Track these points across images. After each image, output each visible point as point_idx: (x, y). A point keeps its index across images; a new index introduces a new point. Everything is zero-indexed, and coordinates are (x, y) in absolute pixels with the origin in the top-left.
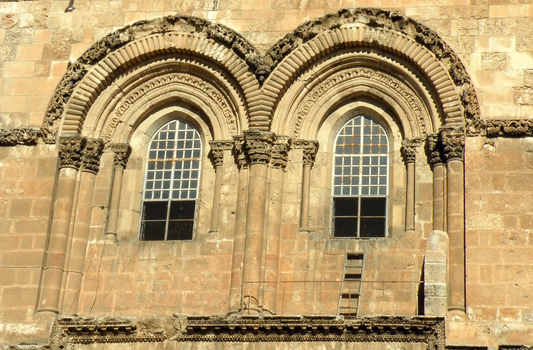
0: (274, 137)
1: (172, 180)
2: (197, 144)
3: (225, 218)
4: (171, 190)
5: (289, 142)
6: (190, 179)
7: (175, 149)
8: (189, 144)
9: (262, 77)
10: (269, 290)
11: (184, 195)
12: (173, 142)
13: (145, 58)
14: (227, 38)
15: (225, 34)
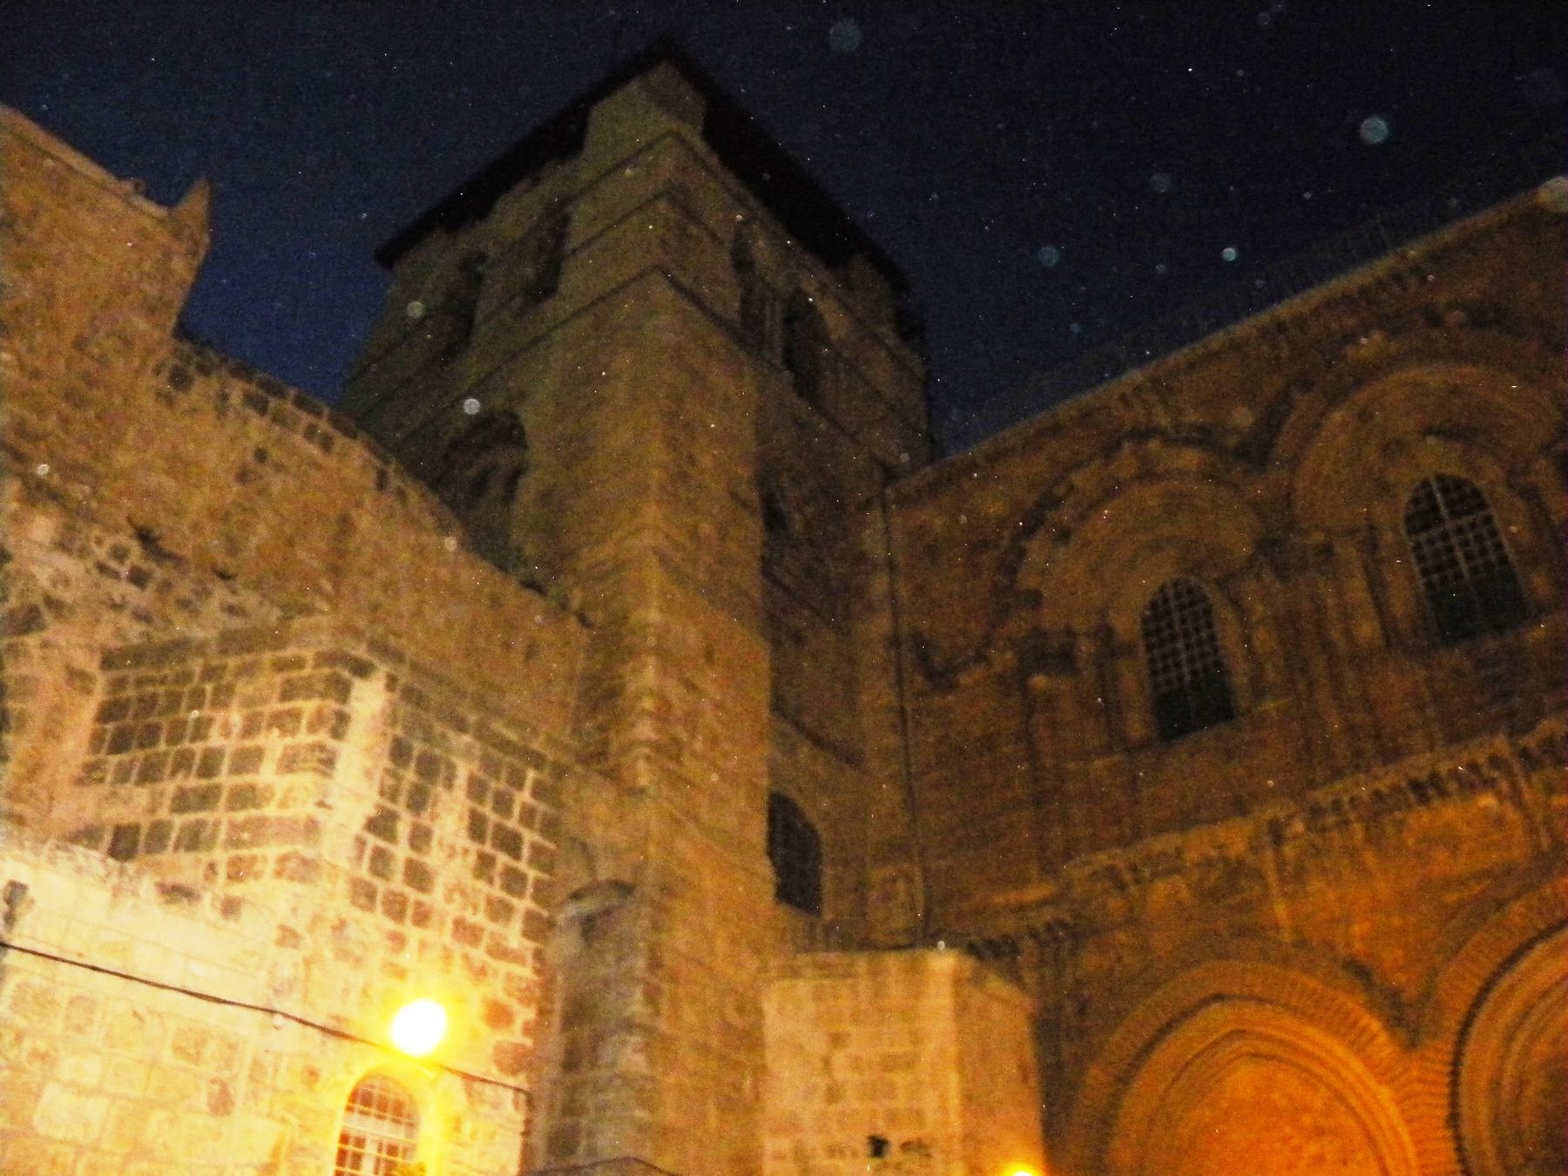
4: (1185, 670)
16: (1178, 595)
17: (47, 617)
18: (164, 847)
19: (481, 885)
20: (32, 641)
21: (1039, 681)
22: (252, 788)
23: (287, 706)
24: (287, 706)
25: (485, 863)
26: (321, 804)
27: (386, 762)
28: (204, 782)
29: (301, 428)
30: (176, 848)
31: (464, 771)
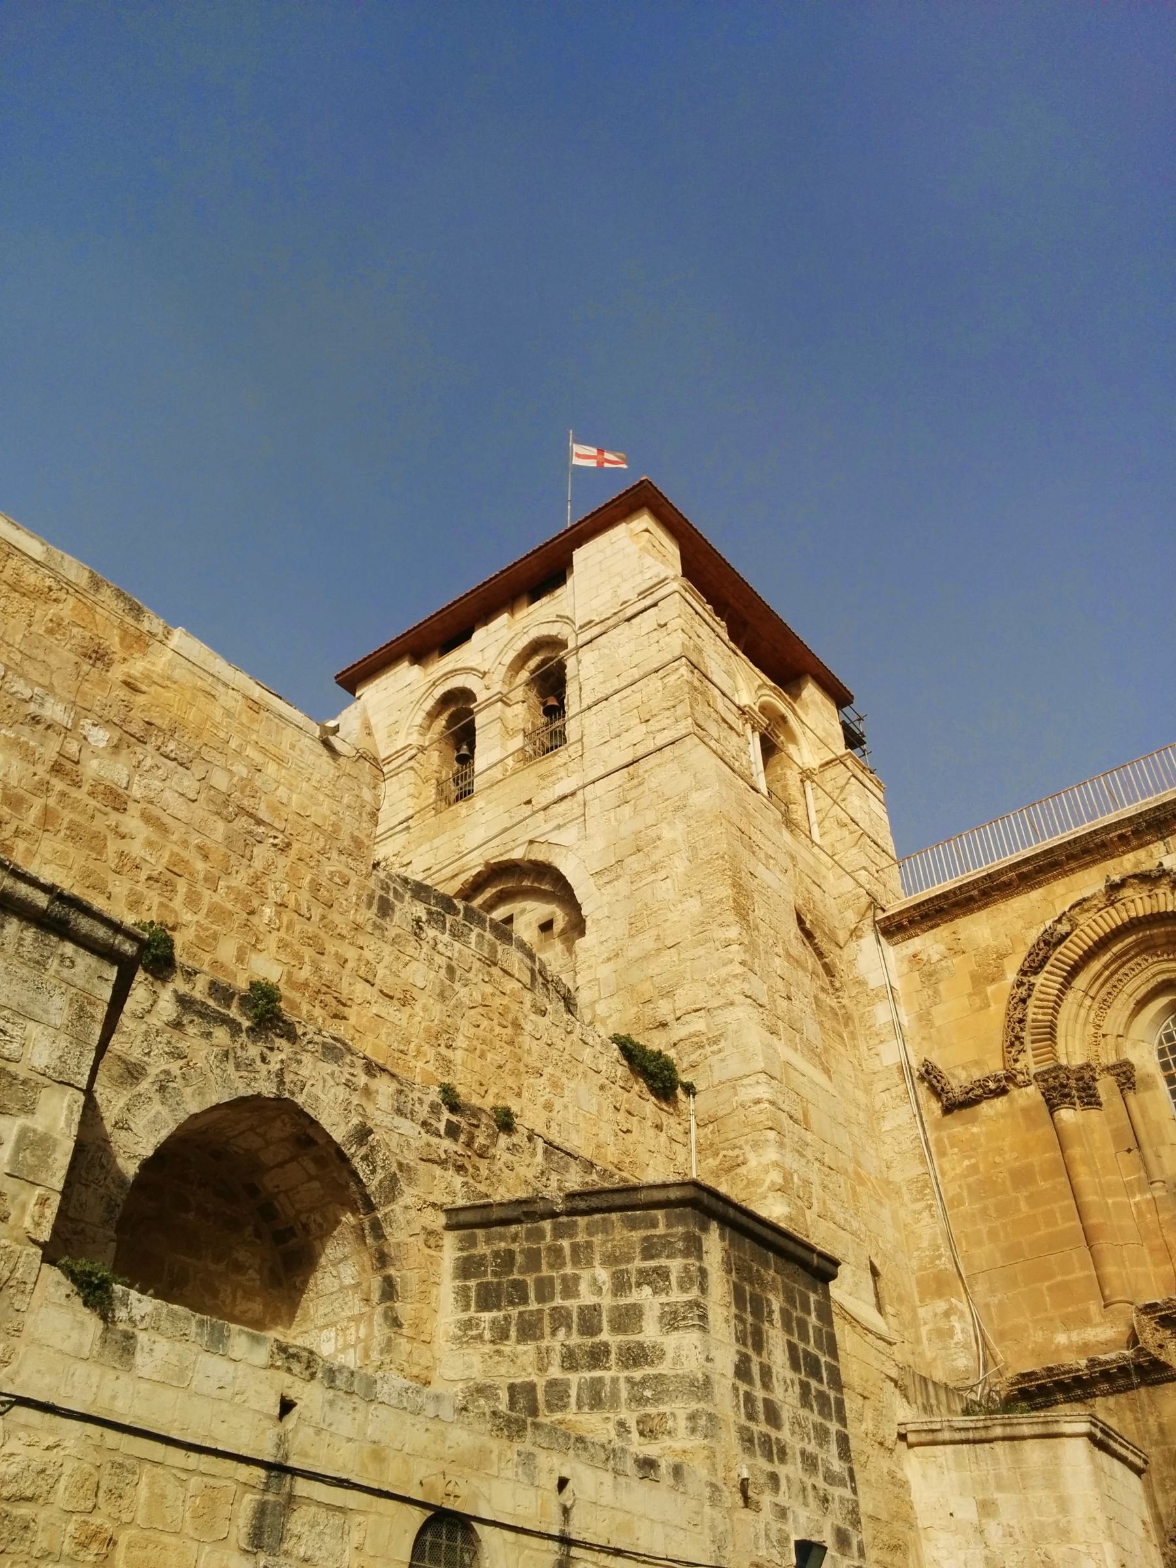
13: (1102, 944)
17: (402, 1183)
18: (565, 1406)
20: (397, 1207)
21: (1066, 1115)
22: (640, 1345)
23: (652, 1263)
24: (652, 1263)
25: (805, 1387)
26: (708, 1359)
27: (733, 1310)
28: (589, 1341)
29: (473, 937)
30: (579, 1408)
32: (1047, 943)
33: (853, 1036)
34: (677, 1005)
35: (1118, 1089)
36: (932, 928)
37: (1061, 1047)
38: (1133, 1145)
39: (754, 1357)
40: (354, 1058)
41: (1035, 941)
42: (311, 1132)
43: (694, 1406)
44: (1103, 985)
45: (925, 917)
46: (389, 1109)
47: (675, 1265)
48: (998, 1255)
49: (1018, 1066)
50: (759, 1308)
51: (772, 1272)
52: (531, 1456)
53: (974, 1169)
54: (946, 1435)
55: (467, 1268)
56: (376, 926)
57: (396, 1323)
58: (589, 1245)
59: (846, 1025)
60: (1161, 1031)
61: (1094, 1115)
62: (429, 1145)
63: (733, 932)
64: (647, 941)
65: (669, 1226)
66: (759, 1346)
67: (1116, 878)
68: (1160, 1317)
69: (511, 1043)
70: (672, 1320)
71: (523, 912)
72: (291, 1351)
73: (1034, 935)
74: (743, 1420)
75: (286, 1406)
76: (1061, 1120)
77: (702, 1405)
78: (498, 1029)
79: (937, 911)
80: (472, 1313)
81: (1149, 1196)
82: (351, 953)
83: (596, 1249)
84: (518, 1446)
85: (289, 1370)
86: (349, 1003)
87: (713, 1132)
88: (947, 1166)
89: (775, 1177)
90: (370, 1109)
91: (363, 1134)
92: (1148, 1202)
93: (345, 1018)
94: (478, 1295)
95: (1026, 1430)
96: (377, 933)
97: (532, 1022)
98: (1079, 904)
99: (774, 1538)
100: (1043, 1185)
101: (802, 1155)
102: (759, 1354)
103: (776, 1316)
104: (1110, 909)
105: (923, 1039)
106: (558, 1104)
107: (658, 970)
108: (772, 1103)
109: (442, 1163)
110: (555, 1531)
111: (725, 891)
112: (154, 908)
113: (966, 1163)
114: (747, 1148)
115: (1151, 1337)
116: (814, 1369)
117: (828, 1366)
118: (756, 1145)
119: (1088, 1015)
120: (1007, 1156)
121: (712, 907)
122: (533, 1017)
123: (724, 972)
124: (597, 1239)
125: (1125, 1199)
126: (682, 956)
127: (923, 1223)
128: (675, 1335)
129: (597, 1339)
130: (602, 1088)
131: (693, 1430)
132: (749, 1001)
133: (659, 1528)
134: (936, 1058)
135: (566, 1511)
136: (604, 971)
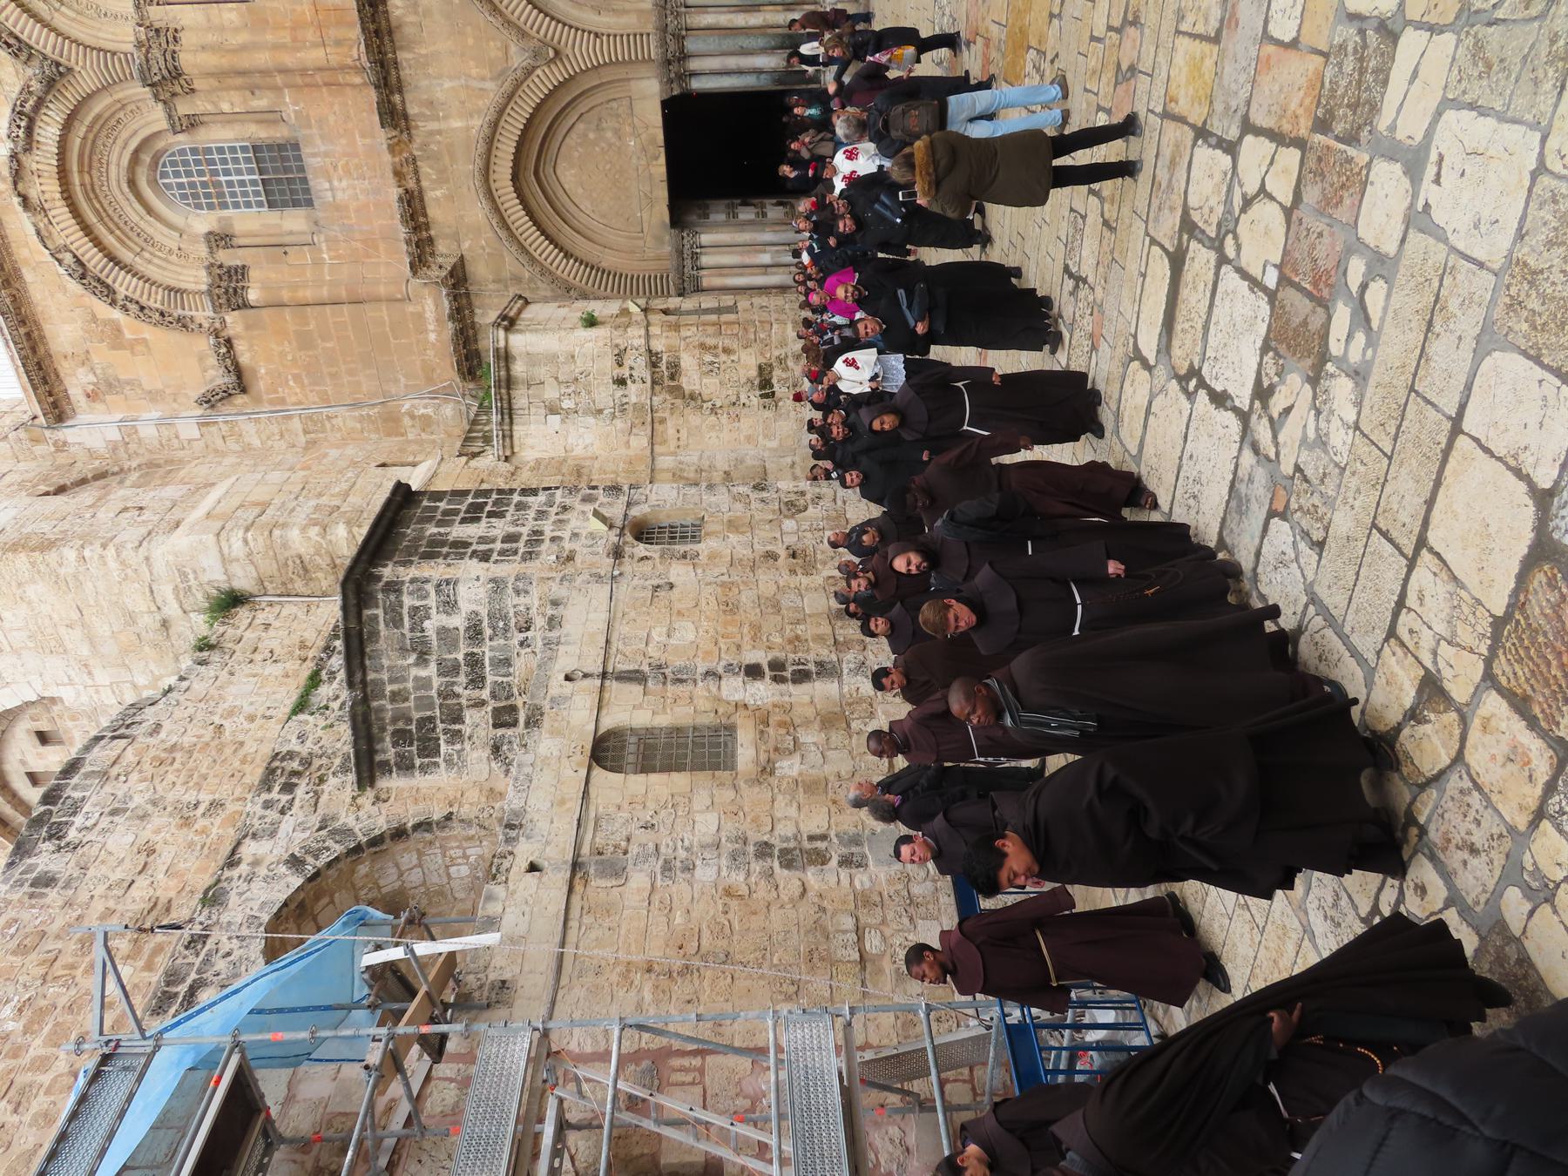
0: (139, 45)
1: (234, 178)
2: (182, 152)
3: (261, 103)
4: (246, 177)
5: (141, 26)
6: (228, 156)
7: (196, 179)
8: (185, 163)
9: (61, 69)
10: (333, 33)
11: (247, 160)
12: (189, 183)
13: (87, 230)
14: (23, 124)
15: (19, 127)
16: (177, 174)
17: (337, 825)
19: (508, 516)
21: (253, 296)
22: (468, 629)
23: (406, 619)
25: (491, 515)
26: (478, 579)
27: (440, 560)
28: (464, 669)
30: (510, 675)
31: (435, 530)
32: (83, 277)
33: (170, 462)
34: (144, 609)
35: (231, 250)
36: (58, 376)
37: (191, 287)
38: (282, 250)
39: (474, 547)
40: (223, 878)
41: (81, 287)
42: (292, 906)
43: (510, 591)
44: (129, 238)
45: (46, 383)
46: (272, 842)
47: (408, 601)
48: (368, 372)
49: (206, 325)
50: (437, 542)
51: (409, 531)
52: (553, 700)
53: (297, 378)
54: (506, 427)
55: (405, 766)
56: (67, 886)
57: (449, 817)
58: (390, 669)
59: (159, 466)
60: (178, 201)
61: (253, 274)
62: (302, 807)
63: (70, 554)
64: (73, 638)
65: (377, 607)
66: (466, 545)
67: (16, 200)
68: (420, 261)
69: (190, 753)
70: (449, 606)
71: (23, 762)
72: (494, 871)
73: (74, 286)
74: (518, 558)
75: (533, 868)
76: (257, 301)
77: (510, 586)
78: (177, 765)
79: (40, 369)
80: (440, 760)
81: (324, 247)
82: (99, 907)
83: (393, 664)
84: (546, 709)
85: (508, 870)
86: (153, 900)
87: (271, 582)
88: (294, 399)
89: (314, 532)
90: (271, 858)
91: (295, 862)
92: (329, 249)
93: (170, 901)
94: (427, 756)
95: (503, 373)
96: (74, 885)
97: (169, 735)
98: (42, 241)
99: (591, 543)
100: (311, 327)
101: (293, 510)
102: (471, 544)
103: (442, 530)
104: (50, 214)
105: (175, 400)
106: (248, 709)
107: (106, 627)
108: (247, 530)
109: (317, 795)
110: (598, 682)
111: (22, 560)
112: (52, 1098)
113: (291, 383)
114: (287, 554)
115: (435, 273)
116: (478, 508)
117: (475, 497)
118: (285, 546)
119: (160, 258)
120: (287, 349)
121: (39, 572)
122: (163, 735)
123: (113, 564)
124: (385, 662)
125: (326, 266)
126: (92, 603)
127: (341, 424)
128: (460, 603)
129: (462, 662)
130: (232, 674)
131: (527, 592)
132: (145, 543)
133: (591, 616)
134: (196, 394)
135: (586, 676)
136: (102, 677)
